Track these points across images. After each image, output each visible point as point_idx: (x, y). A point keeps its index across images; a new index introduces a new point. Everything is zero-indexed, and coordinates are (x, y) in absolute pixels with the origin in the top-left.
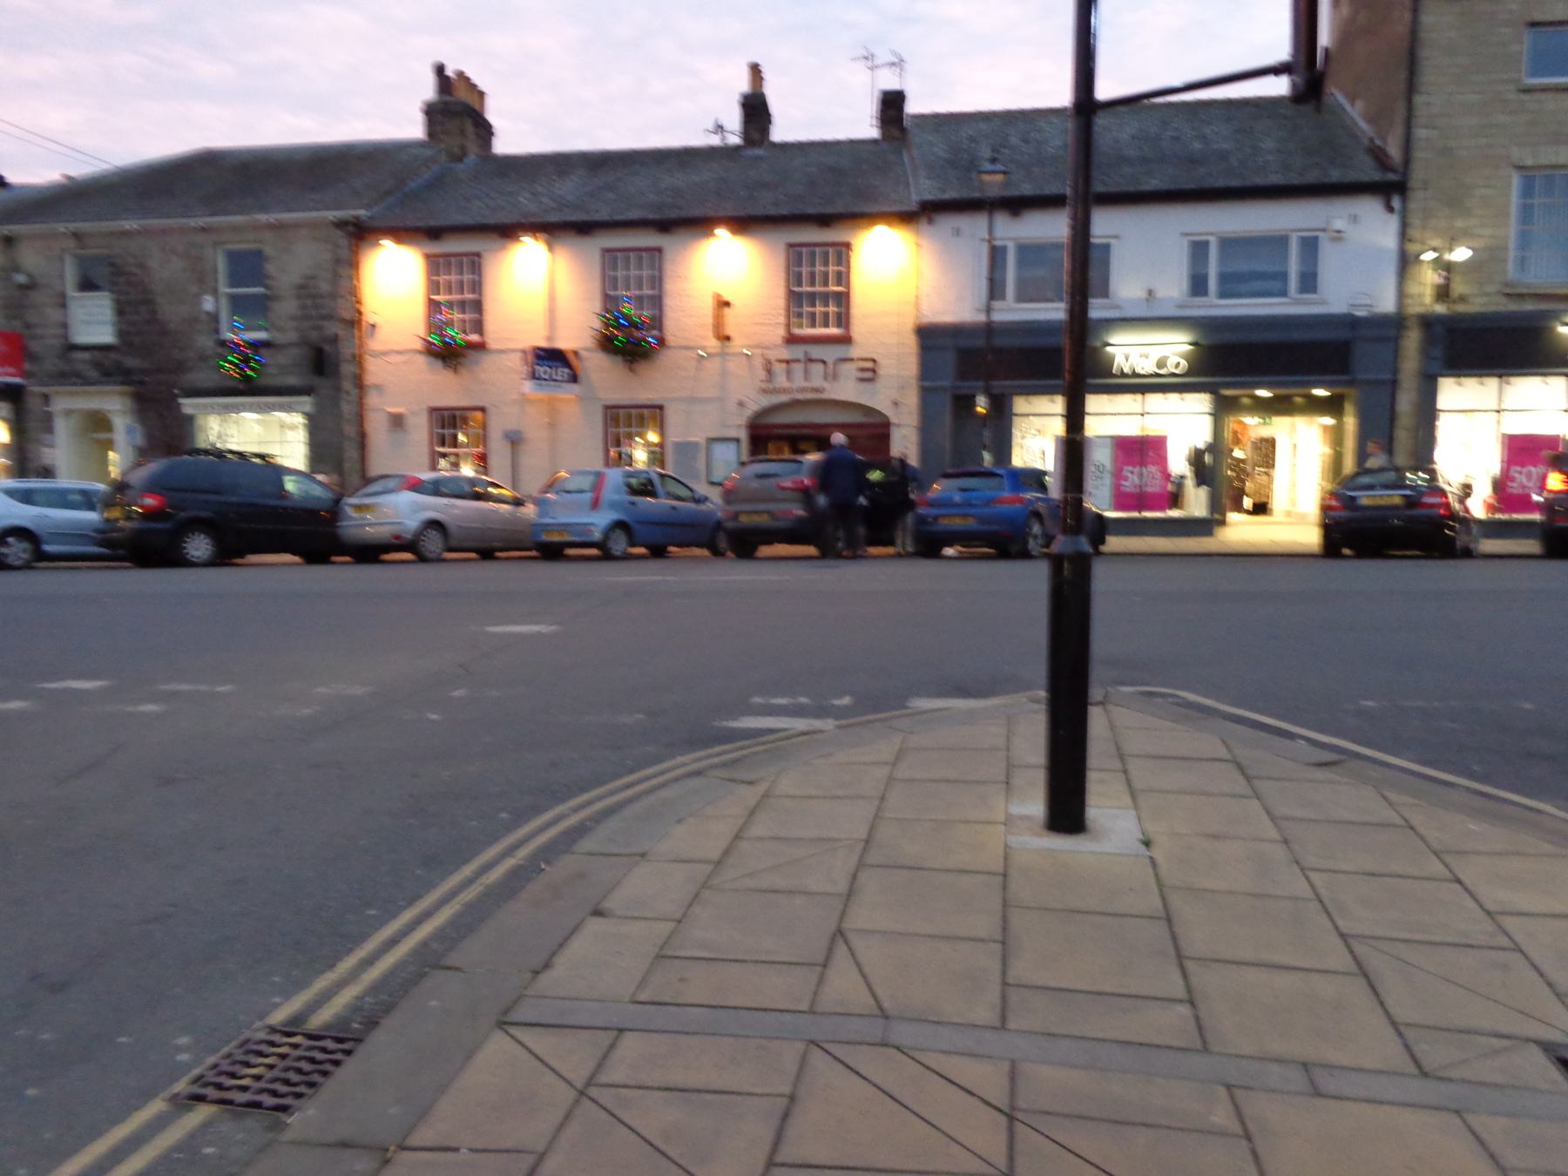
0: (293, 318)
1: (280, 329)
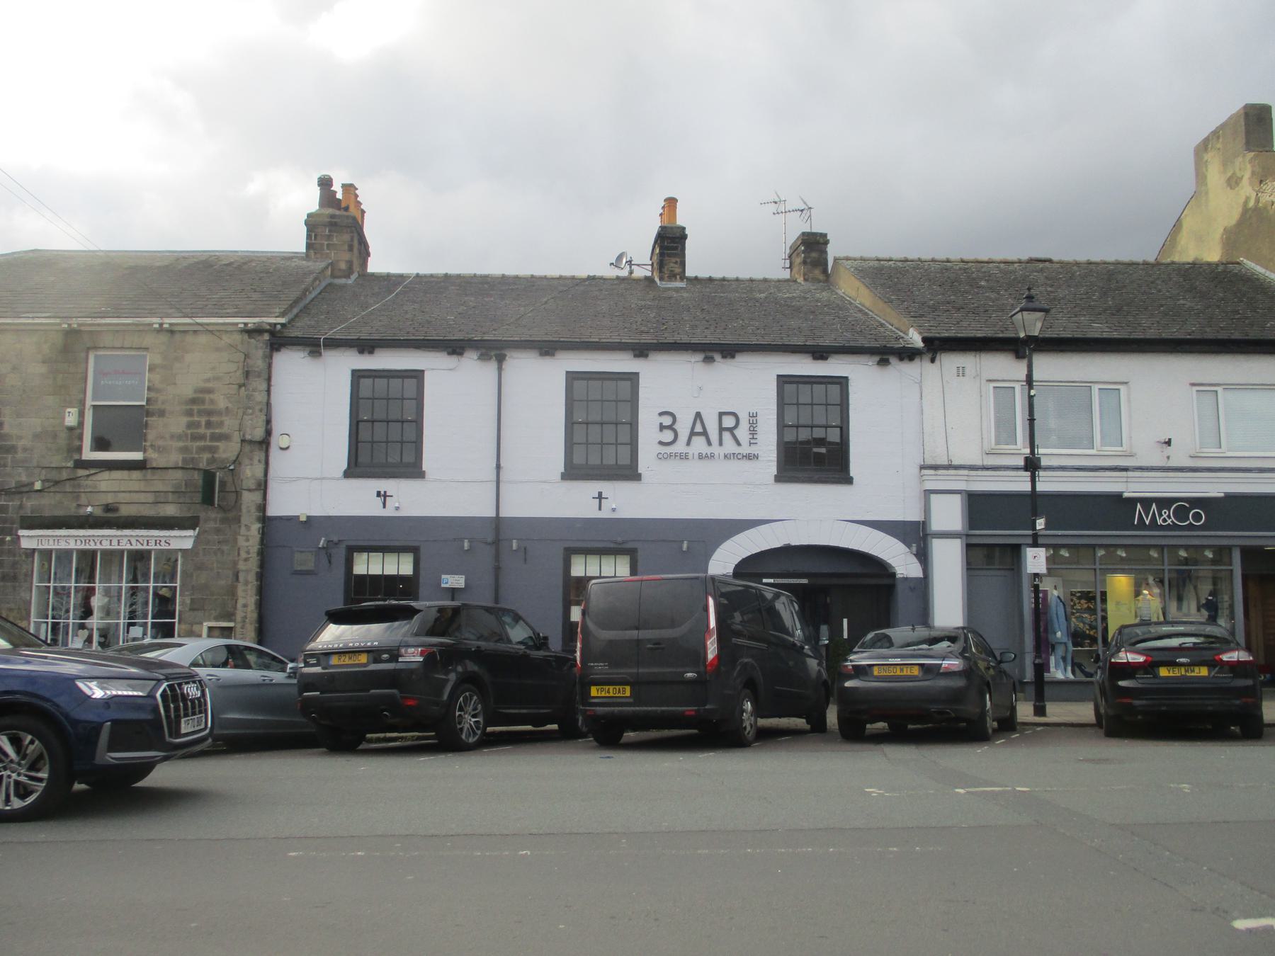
0: (179, 437)
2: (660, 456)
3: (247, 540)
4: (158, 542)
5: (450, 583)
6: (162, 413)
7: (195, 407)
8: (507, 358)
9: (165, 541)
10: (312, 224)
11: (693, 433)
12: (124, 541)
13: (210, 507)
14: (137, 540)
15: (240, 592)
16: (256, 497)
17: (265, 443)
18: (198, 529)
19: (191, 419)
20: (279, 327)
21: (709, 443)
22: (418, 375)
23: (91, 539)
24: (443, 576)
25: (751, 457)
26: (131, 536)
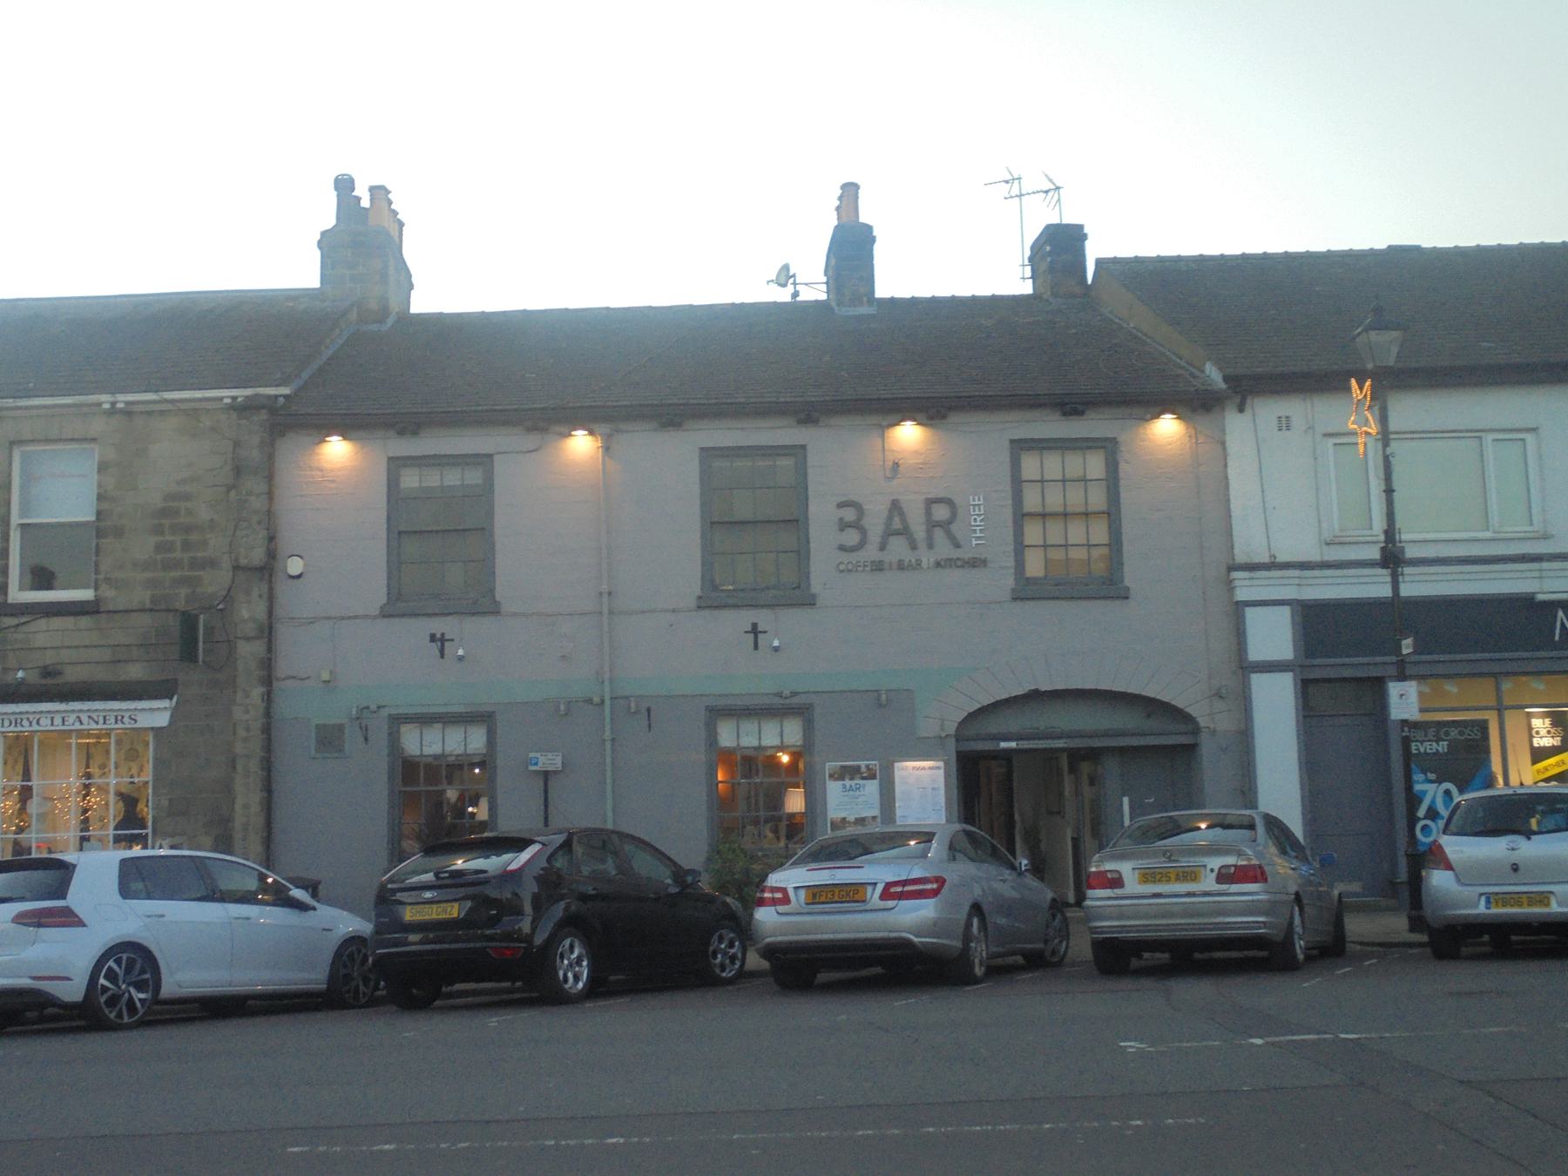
2: (842, 567)
4: (119, 718)
5: (540, 764)
6: (119, 532)
7: (166, 522)
9: (130, 717)
10: (328, 243)
11: (889, 533)
12: (72, 718)
14: (89, 717)
15: (238, 786)
16: (257, 648)
17: (268, 569)
20: (281, 400)
21: (914, 547)
23: (22, 716)
25: (976, 563)
26: (81, 711)
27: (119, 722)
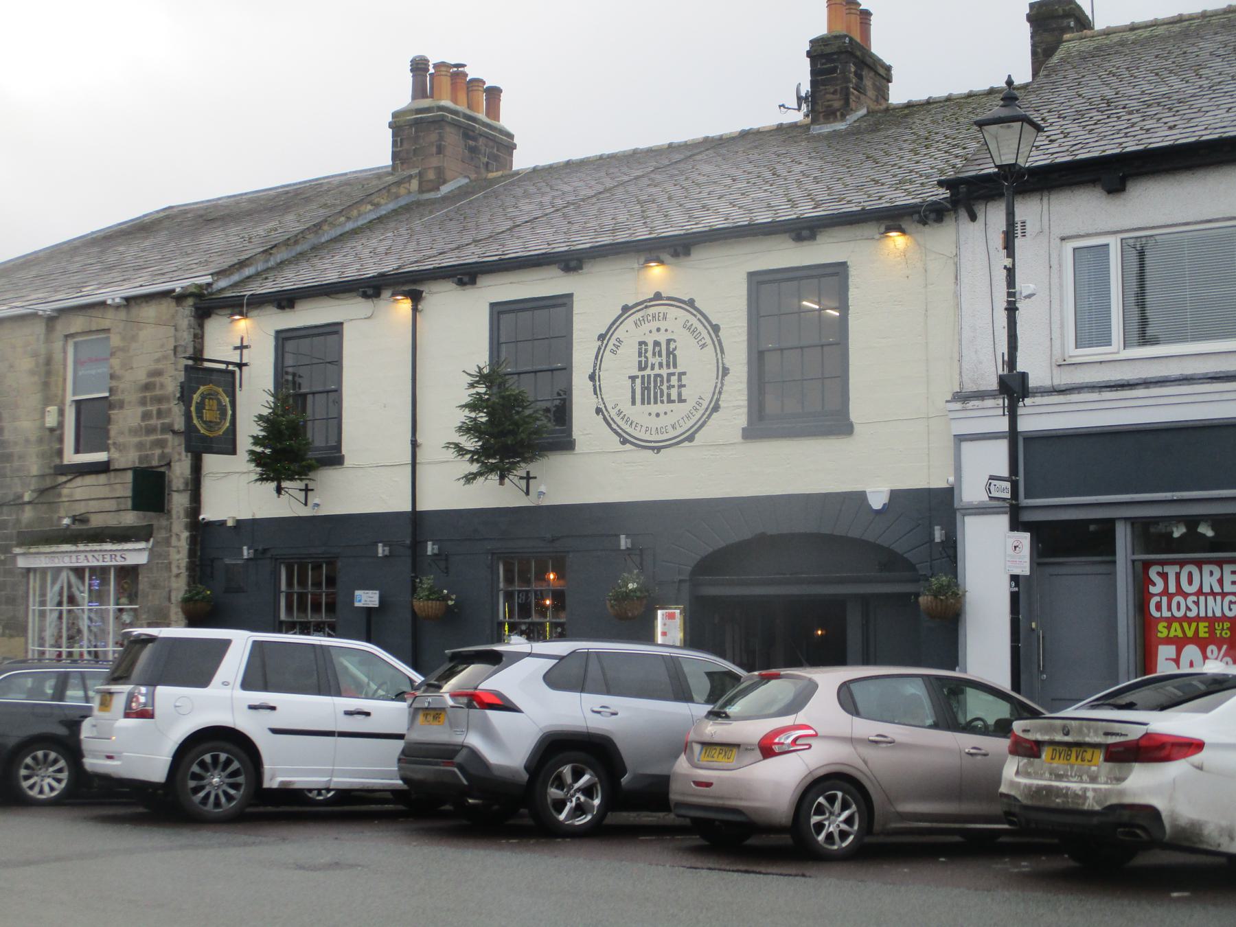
0: (134, 432)
1: (121, 448)
3: (179, 552)
4: (113, 556)
5: (363, 602)
6: (121, 404)
7: (148, 394)
8: (424, 294)
13: (161, 514)
14: (93, 556)
18: (152, 540)
19: (144, 409)
22: (335, 330)
24: (358, 593)
27: (113, 560)
